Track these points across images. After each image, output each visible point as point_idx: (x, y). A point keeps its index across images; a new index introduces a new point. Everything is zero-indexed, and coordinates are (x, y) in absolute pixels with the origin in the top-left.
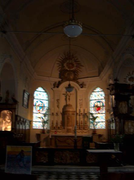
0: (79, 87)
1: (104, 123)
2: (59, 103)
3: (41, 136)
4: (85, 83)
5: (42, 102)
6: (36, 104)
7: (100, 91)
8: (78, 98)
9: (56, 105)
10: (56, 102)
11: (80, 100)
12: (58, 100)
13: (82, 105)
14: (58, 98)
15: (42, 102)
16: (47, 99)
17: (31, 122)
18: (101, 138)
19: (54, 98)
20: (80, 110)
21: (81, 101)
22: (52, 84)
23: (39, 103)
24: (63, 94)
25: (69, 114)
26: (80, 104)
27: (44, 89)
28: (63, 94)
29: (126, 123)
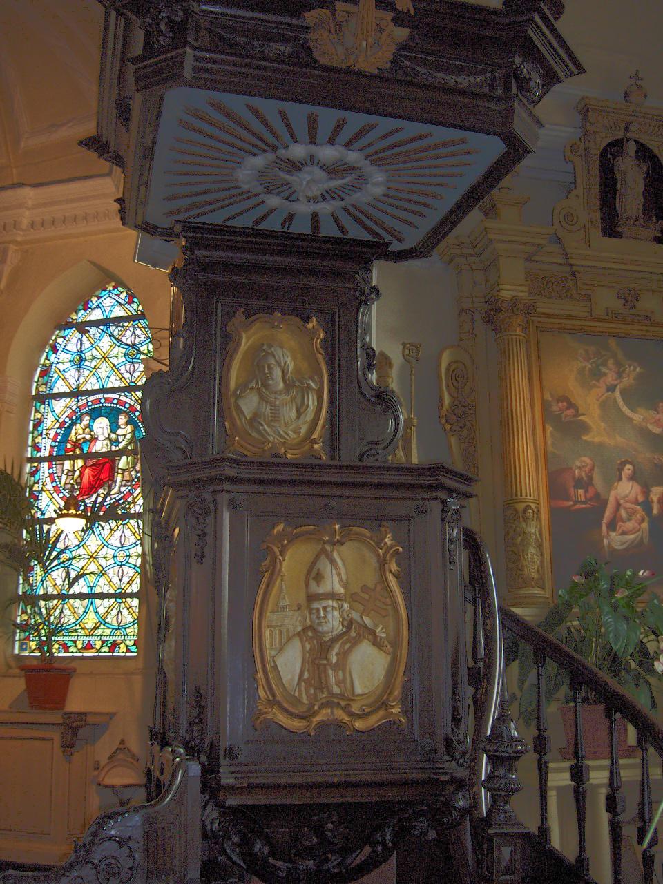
1: (135, 602)
7: (119, 312)
18: (103, 749)
29: (293, 560)
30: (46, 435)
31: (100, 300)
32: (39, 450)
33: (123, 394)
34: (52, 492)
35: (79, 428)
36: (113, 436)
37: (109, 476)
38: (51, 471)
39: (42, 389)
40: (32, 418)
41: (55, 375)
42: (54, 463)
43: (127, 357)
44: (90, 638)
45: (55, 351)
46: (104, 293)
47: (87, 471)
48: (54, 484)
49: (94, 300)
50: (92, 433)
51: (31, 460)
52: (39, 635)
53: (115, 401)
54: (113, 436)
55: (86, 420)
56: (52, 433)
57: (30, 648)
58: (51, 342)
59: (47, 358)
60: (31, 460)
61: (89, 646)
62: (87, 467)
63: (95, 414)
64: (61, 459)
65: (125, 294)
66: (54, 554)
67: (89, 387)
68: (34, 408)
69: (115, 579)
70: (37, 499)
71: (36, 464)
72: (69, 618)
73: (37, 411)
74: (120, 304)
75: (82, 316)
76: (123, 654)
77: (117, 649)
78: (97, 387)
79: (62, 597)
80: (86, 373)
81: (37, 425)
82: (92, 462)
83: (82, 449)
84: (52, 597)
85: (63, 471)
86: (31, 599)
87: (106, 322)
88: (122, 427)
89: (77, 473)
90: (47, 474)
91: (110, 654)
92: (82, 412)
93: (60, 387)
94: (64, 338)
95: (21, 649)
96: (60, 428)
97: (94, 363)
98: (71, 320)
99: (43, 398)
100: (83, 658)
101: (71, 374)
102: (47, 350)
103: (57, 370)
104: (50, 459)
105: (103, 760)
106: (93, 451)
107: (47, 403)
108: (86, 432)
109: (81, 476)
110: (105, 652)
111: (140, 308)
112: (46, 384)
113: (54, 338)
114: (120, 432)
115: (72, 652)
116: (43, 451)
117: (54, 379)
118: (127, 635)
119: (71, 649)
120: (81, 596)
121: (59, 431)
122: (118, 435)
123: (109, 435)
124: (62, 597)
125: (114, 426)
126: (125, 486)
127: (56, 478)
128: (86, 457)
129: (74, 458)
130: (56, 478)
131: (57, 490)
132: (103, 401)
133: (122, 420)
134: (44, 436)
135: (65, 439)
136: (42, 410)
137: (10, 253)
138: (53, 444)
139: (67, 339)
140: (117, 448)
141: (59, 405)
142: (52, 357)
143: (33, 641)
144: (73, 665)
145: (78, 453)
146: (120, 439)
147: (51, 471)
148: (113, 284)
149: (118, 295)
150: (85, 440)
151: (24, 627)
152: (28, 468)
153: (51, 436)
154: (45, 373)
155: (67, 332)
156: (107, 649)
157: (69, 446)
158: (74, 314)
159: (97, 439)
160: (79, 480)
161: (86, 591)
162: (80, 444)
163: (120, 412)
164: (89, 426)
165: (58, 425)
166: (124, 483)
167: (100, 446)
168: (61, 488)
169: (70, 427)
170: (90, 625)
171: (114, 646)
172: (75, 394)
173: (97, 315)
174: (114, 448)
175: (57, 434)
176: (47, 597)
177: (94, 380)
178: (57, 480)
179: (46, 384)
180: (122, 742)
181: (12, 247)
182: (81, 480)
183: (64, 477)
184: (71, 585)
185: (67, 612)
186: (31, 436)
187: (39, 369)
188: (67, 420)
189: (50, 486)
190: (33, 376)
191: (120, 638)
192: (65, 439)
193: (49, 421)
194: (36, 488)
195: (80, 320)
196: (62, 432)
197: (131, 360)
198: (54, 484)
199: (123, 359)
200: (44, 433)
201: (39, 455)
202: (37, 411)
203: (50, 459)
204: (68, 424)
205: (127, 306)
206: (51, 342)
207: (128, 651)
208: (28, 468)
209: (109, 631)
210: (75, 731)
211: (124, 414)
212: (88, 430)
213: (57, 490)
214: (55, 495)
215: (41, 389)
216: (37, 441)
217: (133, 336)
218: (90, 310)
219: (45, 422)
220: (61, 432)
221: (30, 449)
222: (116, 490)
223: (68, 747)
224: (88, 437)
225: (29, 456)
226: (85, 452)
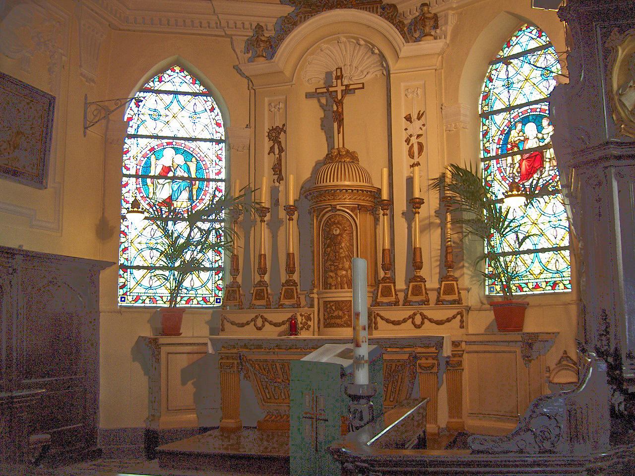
0: (397, 37)
1: (567, 253)
2: (281, 150)
3: (164, 350)
4: (434, 10)
5: (188, 155)
6: (148, 166)
7: (533, 45)
8: (399, 112)
9: (267, 162)
10: (267, 144)
11: (408, 118)
12: (276, 134)
13: (421, 147)
14: (278, 123)
15: (188, 155)
16: (217, 136)
17: (104, 275)
18: (552, 358)
19: (253, 123)
20: (410, 181)
21: (415, 127)
22: (240, 46)
23: (169, 157)
24: (309, 96)
25: (334, 208)
26: (408, 141)
27: (195, 78)
28: (309, 96)
30: (492, 141)
31: (518, 38)
32: (488, 152)
33: (543, 104)
34: (501, 181)
35: (514, 133)
36: (540, 136)
37: (540, 164)
38: (498, 166)
39: (486, 108)
40: (481, 130)
41: (494, 98)
42: (500, 160)
43: (543, 76)
44: (536, 281)
45: (491, 80)
46: (520, 33)
47: (524, 163)
48: (502, 175)
49: (514, 39)
50: (524, 135)
51: (484, 160)
52: (501, 281)
53: (538, 110)
54: (540, 136)
55: (519, 126)
56: (496, 139)
57: (496, 290)
58: (488, 74)
59: (486, 86)
60: (484, 160)
61: (537, 287)
62: (523, 160)
63: (525, 121)
64: (505, 156)
65: (535, 31)
66: (506, 223)
67: (518, 102)
68: (481, 123)
69: (552, 238)
70: (491, 186)
71: (487, 162)
72: (521, 269)
73: (484, 125)
74: (533, 39)
75: (507, 52)
76: (562, 291)
77: (557, 287)
78: (524, 101)
79: (515, 253)
80: (515, 92)
81: (484, 136)
82: (527, 155)
83: (518, 148)
84: (509, 254)
85: (507, 165)
86: (493, 256)
87: (524, 53)
88: (545, 128)
89: (517, 165)
90: (496, 168)
91: (553, 291)
92: (515, 121)
93: (498, 106)
94: (496, 70)
95: (490, 291)
96: (501, 134)
97: (520, 84)
98: (499, 57)
99: (486, 115)
100: (534, 295)
101: (504, 96)
102: (485, 81)
103: (494, 93)
104: (497, 158)
105: (553, 366)
106: (527, 148)
107: (490, 118)
108: (520, 135)
109: (520, 167)
110: (549, 290)
111: (548, 39)
112: (488, 105)
113: (489, 71)
114: (544, 132)
115: (526, 291)
116: (491, 152)
117: (493, 100)
118: (564, 277)
119: (524, 289)
120: (529, 252)
121: (501, 137)
122: (543, 134)
123: (537, 135)
124: (515, 253)
125: (540, 128)
126: (552, 170)
127: (503, 170)
128: (521, 152)
129: (515, 154)
130: (503, 170)
131: (504, 178)
132: (529, 111)
133: (545, 122)
134: (491, 142)
135: (506, 142)
136: (487, 124)
137: (450, 17)
138: (498, 146)
139: (498, 70)
140: (544, 144)
141: (498, 118)
142: (490, 85)
143: (497, 285)
144: (527, 300)
145: (516, 150)
146: (545, 136)
147: (498, 166)
148: (526, 25)
149: (531, 33)
150: (521, 141)
151: (490, 276)
152: (482, 165)
153: (496, 141)
154: (486, 97)
155: (498, 65)
156: (550, 288)
157: (509, 146)
158: (501, 51)
159: (528, 139)
160: (519, 170)
161: (532, 248)
162: (517, 144)
163: (542, 117)
164: (521, 131)
165: (500, 132)
166: (551, 168)
167: (532, 144)
168: (507, 177)
169: (509, 133)
170: (537, 272)
171: (555, 284)
172: (509, 109)
173: (517, 50)
174: (541, 144)
175: (500, 139)
176: (504, 254)
177: (521, 96)
178: (504, 172)
179: (488, 105)
180: (565, 352)
181: (451, 12)
182: (520, 169)
183: (508, 169)
184: (520, 244)
185: (519, 263)
186: (482, 143)
187: (482, 95)
188: (506, 128)
189: (499, 177)
190: (478, 102)
191: (559, 279)
192: (506, 142)
193: (493, 131)
194: (489, 178)
195: (506, 56)
196: (503, 137)
197: (546, 78)
198: (502, 175)
199: (541, 78)
200: (491, 140)
201: (489, 155)
202: (484, 125)
203: (497, 158)
204: (506, 131)
205: (538, 39)
206: (488, 74)
207: (566, 288)
208: (482, 165)
209: (551, 275)
210: (530, 346)
211: (546, 118)
212: (521, 133)
213: (504, 178)
214: (503, 182)
215: (484, 109)
216: (486, 145)
217: (545, 60)
218: (512, 47)
219: (490, 132)
220: (502, 137)
221: (482, 152)
222: (546, 174)
223: (527, 358)
224: (522, 138)
225: (482, 157)
226: (521, 149)
